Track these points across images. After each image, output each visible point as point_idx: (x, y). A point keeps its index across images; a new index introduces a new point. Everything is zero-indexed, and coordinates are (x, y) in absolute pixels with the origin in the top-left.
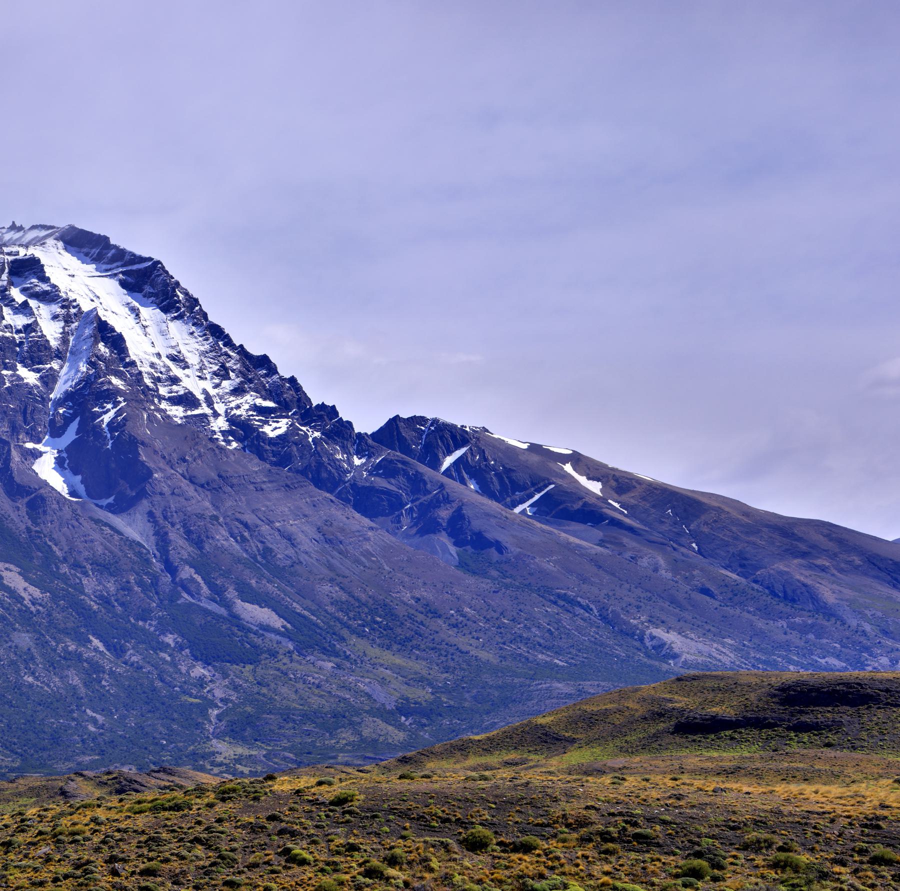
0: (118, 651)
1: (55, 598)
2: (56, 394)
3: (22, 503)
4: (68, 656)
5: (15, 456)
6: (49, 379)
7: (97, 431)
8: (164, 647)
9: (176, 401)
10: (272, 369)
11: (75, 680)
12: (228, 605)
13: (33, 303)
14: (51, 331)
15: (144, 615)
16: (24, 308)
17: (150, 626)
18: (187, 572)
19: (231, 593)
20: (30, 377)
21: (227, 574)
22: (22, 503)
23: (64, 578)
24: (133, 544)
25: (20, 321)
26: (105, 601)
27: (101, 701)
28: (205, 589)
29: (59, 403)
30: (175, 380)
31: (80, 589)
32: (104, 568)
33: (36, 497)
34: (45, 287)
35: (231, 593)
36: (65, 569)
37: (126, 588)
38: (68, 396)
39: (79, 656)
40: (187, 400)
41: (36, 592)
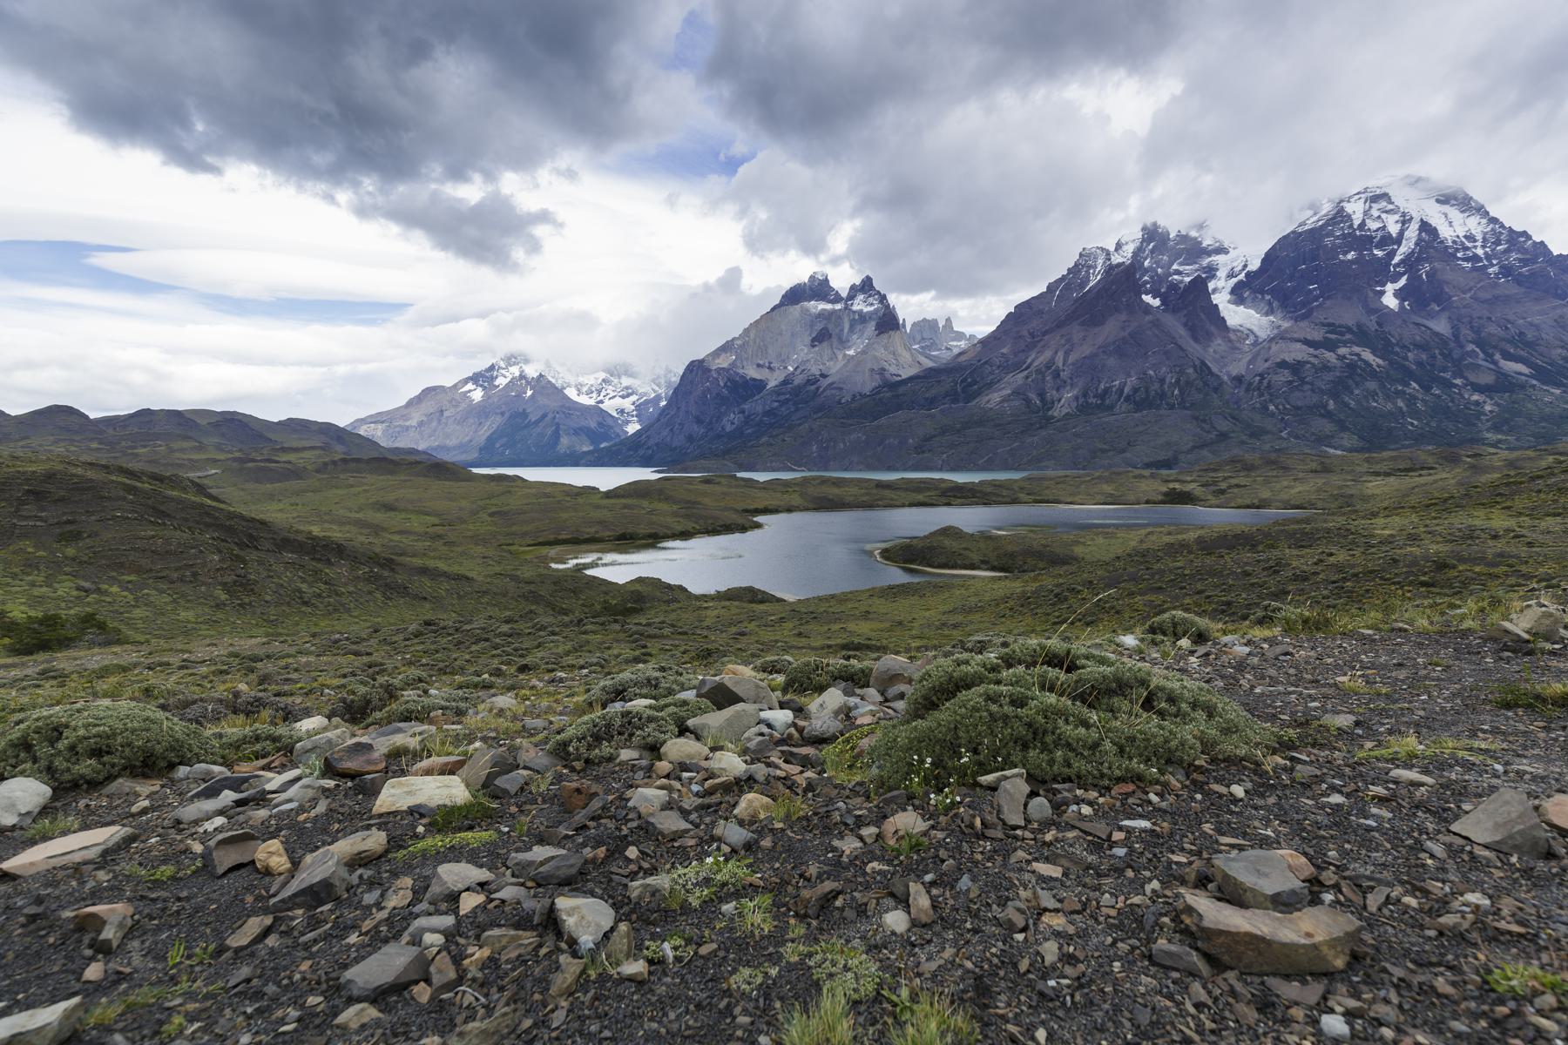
1: (1391, 363)
2: (1397, 259)
4: (1397, 393)
5: (1371, 294)
6: (1392, 254)
9: (1466, 259)
10: (1529, 237)
11: (1400, 404)
12: (1495, 363)
13: (1384, 216)
14: (1394, 229)
15: (1444, 370)
17: (1448, 375)
18: (1471, 347)
19: (1497, 356)
20: (1379, 253)
21: (1495, 347)
23: (1397, 354)
24: (1437, 334)
26: (1420, 364)
27: (1415, 413)
29: (1397, 265)
30: (1467, 249)
31: (1406, 359)
34: (1391, 207)
35: (1497, 356)
36: (1397, 349)
37: (1434, 357)
38: (1402, 261)
39: (1404, 392)
41: (1380, 362)
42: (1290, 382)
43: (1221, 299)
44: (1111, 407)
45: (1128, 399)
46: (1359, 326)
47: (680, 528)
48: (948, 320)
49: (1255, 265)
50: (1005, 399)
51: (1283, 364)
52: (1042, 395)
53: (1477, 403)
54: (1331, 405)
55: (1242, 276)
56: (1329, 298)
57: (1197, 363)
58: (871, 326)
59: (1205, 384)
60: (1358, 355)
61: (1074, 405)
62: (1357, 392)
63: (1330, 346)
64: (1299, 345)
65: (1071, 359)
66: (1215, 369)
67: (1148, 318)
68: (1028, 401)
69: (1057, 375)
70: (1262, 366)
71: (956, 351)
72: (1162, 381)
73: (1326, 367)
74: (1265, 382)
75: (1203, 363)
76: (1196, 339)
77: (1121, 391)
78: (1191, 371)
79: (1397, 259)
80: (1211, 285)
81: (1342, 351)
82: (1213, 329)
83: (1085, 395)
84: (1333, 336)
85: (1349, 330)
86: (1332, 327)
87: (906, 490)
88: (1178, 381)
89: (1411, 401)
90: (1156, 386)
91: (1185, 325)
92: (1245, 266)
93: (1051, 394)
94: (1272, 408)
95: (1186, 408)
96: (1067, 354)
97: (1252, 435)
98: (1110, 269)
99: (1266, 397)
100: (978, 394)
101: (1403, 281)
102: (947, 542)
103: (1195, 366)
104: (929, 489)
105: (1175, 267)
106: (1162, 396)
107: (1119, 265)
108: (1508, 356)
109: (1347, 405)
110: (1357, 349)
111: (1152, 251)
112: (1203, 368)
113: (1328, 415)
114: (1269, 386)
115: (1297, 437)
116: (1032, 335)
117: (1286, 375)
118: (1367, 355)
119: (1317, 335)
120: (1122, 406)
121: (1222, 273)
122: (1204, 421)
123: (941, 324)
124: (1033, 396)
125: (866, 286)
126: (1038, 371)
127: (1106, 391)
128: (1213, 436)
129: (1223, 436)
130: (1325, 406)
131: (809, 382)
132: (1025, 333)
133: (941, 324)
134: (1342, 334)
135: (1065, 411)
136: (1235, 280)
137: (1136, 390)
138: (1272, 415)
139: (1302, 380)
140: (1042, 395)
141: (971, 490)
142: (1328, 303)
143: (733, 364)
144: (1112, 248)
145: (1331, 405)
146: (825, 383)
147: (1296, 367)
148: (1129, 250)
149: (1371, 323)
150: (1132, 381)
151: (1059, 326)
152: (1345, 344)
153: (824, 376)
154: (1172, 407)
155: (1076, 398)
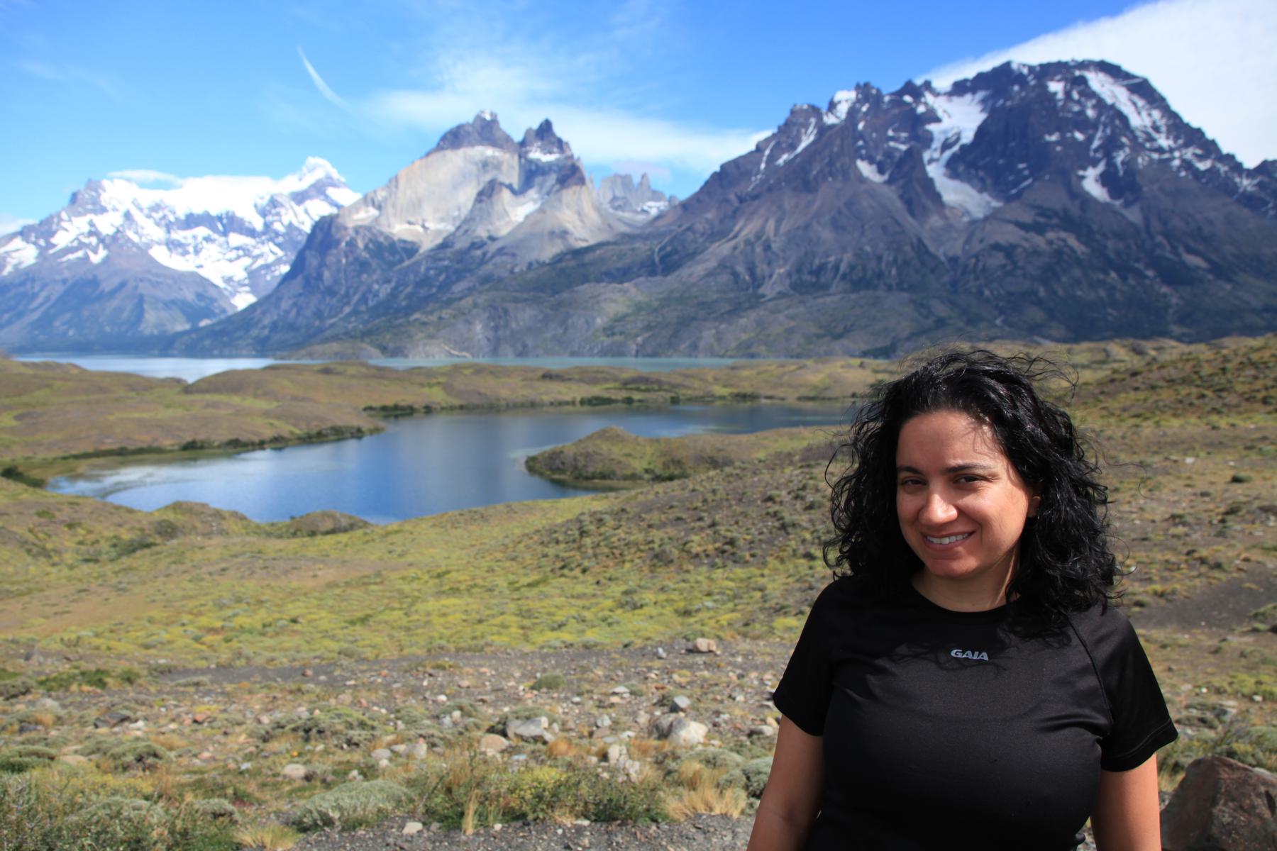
0: (1124, 279)
2: (1096, 143)
3: (1077, 202)
6: (1090, 139)
7: (1115, 166)
8: (1146, 277)
12: (1178, 255)
14: (1090, 113)
15: (1138, 260)
16: (1078, 102)
17: (1140, 266)
18: (1159, 239)
19: (1181, 250)
22: (1077, 202)
24: (1132, 224)
25: (1076, 108)
26: (1118, 253)
28: (1168, 248)
29: (1096, 151)
32: (1119, 236)
33: (1086, 200)
35: (1181, 250)
40: (1160, 150)
42: (1004, 266)
43: (935, 171)
44: (825, 287)
45: (844, 277)
46: (1065, 211)
47: (268, 433)
48: (644, 176)
49: (968, 137)
50: (710, 274)
51: (997, 247)
52: (751, 270)
53: (1165, 296)
54: (1042, 292)
55: (956, 148)
56: (1035, 180)
57: (915, 240)
58: (552, 179)
59: (923, 264)
60: (1064, 241)
61: (788, 281)
62: (1064, 279)
63: (1039, 229)
64: (1011, 227)
65: (784, 228)
66: (932, 249)
67: (864, 187)
68: (735, 275)
69: (767, 247)
70: (976, 247)
71: (654, 212)
72: (879, 258)
73: (1036, 252)
74: (980, 265)
75: (920, 240)
76: (912, 214)
77: (836, 268)
78: (907, 248)
79: (1096, 143)
80: (926, 156)
81: (1051, 235)
82: (929, 204)
83: (799, 271)
84: (1042, 220)
85: (1056, 214)
86: (1042, 211)
87: (581, 380)
88: (895, 260)
89: (1111, 289)
90: (873, 264)
91: (901, 197)
92: (958, 139)
93: (761, 268)
94: (987, 293)
95: (903, 290)
96: (779, 222)
97: (970, 322)
98: (823, 130)
99: (982, 281)
100: (677, 266)
101: (1101, 167)
102: (605, 447)
103: (913, 247)
104: (606, 380)
105: (890, 133)
106: (880, 275)
107: (832, 126)
108: (1190, 251)
109: (1055, 293)
110: (1063, 234)
111: (866, 114)
112: (920, 247)
113: (1040, 303)
114: (984, 269)
115: (1011, 325)
116: (741, 200)
117: (998, 259)
118: (1072, 241)
119: (1027, 217)
120: (837, 286)
121: (936, 144)
122: (922, 305)
123: (636, 180)
124: (740, 269)
125: (545, 131)
126: (748, 242)
127: (822, 267)
128: (930, 322)
129: (941, 323)
130: (1036, 293)
131: (474, 246)
132: (732, 197)
133: (636, 180)
134: (1050, 218)
135: (778, 288)
136: (948, 154)
137: (852, 268)
138: (987, 301)
139: (1015, 263)
140: (751, 270)
141: (658, 382)
142: (1037, 184)
143: (376, 219)
144: (824, 107)
145: (1042, 292)
146: (493, 247)
147: (1008, 251)
148: (843, 110)
149: (1075, 210)
150: (848, 258)
151: (770, 189)
152: (1053, 227)
153: (492, 239)
154: (889, 288)
155: (789, 275)
